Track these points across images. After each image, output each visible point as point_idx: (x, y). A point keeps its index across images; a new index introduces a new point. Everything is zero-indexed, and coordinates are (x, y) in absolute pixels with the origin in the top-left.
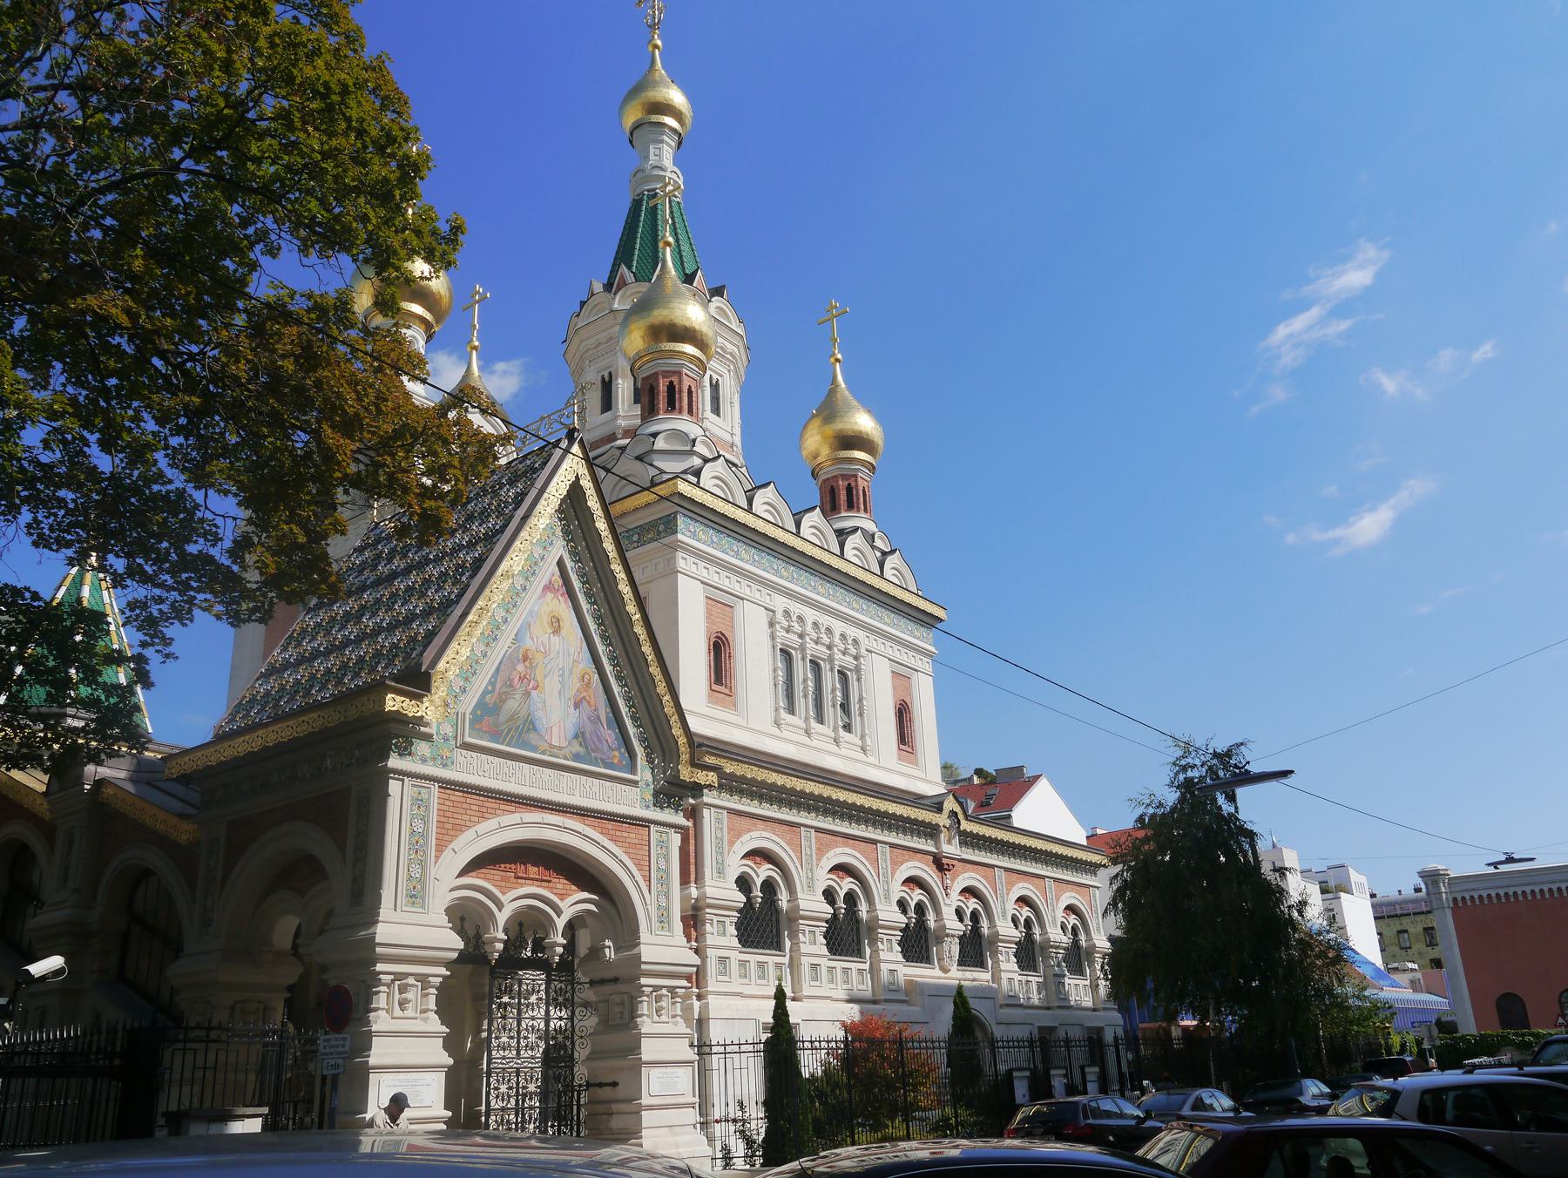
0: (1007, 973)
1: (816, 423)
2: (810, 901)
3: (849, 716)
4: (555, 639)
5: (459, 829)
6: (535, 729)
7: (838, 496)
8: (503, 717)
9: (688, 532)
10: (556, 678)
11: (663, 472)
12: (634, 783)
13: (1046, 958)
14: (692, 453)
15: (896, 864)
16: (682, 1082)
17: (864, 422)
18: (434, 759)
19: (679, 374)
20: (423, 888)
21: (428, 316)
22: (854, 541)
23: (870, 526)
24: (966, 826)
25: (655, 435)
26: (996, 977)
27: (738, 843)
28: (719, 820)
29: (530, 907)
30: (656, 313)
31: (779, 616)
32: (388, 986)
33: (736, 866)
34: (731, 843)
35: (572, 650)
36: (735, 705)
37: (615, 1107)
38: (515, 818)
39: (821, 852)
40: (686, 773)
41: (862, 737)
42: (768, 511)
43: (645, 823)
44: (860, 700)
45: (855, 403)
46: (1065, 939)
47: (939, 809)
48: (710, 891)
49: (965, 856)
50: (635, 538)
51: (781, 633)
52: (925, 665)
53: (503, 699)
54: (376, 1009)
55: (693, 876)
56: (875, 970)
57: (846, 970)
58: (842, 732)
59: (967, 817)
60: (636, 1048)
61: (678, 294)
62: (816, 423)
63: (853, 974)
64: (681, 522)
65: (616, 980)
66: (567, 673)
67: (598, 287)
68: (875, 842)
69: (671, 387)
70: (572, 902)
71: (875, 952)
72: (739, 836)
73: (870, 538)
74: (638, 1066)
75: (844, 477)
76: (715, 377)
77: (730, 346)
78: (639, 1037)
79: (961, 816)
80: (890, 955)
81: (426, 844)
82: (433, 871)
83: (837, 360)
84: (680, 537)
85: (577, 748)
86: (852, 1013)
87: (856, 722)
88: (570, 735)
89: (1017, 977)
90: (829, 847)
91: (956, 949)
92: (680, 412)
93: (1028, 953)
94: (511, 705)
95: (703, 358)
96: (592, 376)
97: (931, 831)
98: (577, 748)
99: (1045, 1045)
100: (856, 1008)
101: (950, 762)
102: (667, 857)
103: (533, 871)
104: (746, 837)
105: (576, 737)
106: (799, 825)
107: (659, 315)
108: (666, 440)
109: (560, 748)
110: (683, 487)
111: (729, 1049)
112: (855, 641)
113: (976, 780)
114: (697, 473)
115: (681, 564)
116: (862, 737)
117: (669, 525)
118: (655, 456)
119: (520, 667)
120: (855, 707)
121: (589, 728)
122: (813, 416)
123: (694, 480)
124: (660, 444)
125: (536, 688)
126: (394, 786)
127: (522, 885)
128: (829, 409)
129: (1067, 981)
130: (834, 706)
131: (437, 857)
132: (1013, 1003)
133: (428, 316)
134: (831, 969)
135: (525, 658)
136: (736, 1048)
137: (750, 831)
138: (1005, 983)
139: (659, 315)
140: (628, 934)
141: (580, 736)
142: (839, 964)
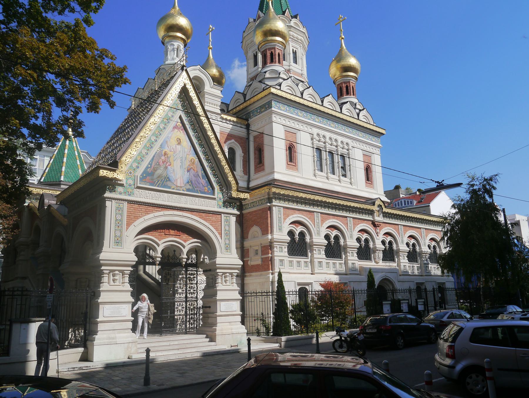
0: (403, 262)
1: (334, 63)
2: (318, 238)
3: (345, 172)
4: (179, 147)
5: (137, 218)
6: (169, 180)
7: (343, 90)
8: (155, 176)
9: (276, 107)
10: (179, 161)
11: (268, 85)
12: (214, 199)
13: (421, 258)
14: (279, 77)
15: (355, 225)
16: (236, 307)
17: (353, 61)
18: (125, 193)
19: (274, 48)
20: (121, 240)
21: (183, 37)
22: (345, 107)
23: (355, 100)
24: (385, 210)
25: (265, 72)
26: (399, 265)
27: (288, 219)
28: (279, 211)
29: (172, 245)
30: (264, 26)
31: (315, 136)
32: (108, 274)
33: (287, 228)
34: (285, 219)
35: (186, 150)
37: (210, 315)
38: (162, 213)
39: (323, 221)
40: (234, 194)
41: (350, 179)
42: (310, 97)
43: (220, 213)
44: (350, 166)
45: (349, 54)
46: (429, 251)
47: (374, 204)
48: (275, 236)
49: (385, 221)
50: (259, 111)
51: (316, 142)
52: (378, 151)
53: (155, 170)
54: (103, 283)
55: (270, 231)
56: (346, 263)
57: (334, 264)
58: (342, 178)
59: (385, 207)
60: (215, 295)
61: (274, 18)
62: (334, 63)
63: (338, 265)
64: (273, 103)
65: (210, 270)
66: (184, 159)
67: (251, 20)
68: (346, 217)
69: (272, 54)
70: (188, 243)
71: (346, 257)
72: (288, 216)
73: (354, 105)
74: (216, 301)
75: (345, 83)
76: (295, 49)
77: (300, 37)
78: (216, 291)
79: (383, 206)
80: (353, 259)
81: (122, 224)
82: (125, 233)
83: (342, 38)
84: (273, 109)
85: (188, 187)
86: (335, 279)
87: (348, 173)
88: (186, 181)
89: (407, 265)
90: (326, 219)
91: (381, 255)
92: (275, 63)
93: (413, 256)
95: (284, 41)
96: (251, 55)
97: (371, 212)
98: (188, 187)
99: (420, 289)
100: (337, 276)
101: (409, 187)
102: (229, 226)
103: (172, 232)
104: (291, 217)
105: (188, 182)
106: (314, 212)
107: (267, 27)
108: (269, 73)
109: (181, 187)
110: (273, 90)
111: (258, 294)
112: (347, 144)
113: (418, 193)
114: (280, 85)
115: (274, 119)
116: (350, 179)
117: (269, 105)
118: (265, 80)
119: (163, 158)
120: (347, 168)
121: (194, 179)
122: (333, 60)
123: (279, 88)
124: (267, 75)
125: (170, 165)
126: (108, 203)
127: (168, 237)
128: (339, 57)
129: (430, 266)
130: (339, 168)
131: (127, 228)
132: (406, 274)
133: (183, 37)
134: (327, 263)
135: (165, 154)
136: (260, 294)
138: (402, 267)
139: (267, 27)
140: (213, 254)
141: (190, 182)
142: (331, 261)
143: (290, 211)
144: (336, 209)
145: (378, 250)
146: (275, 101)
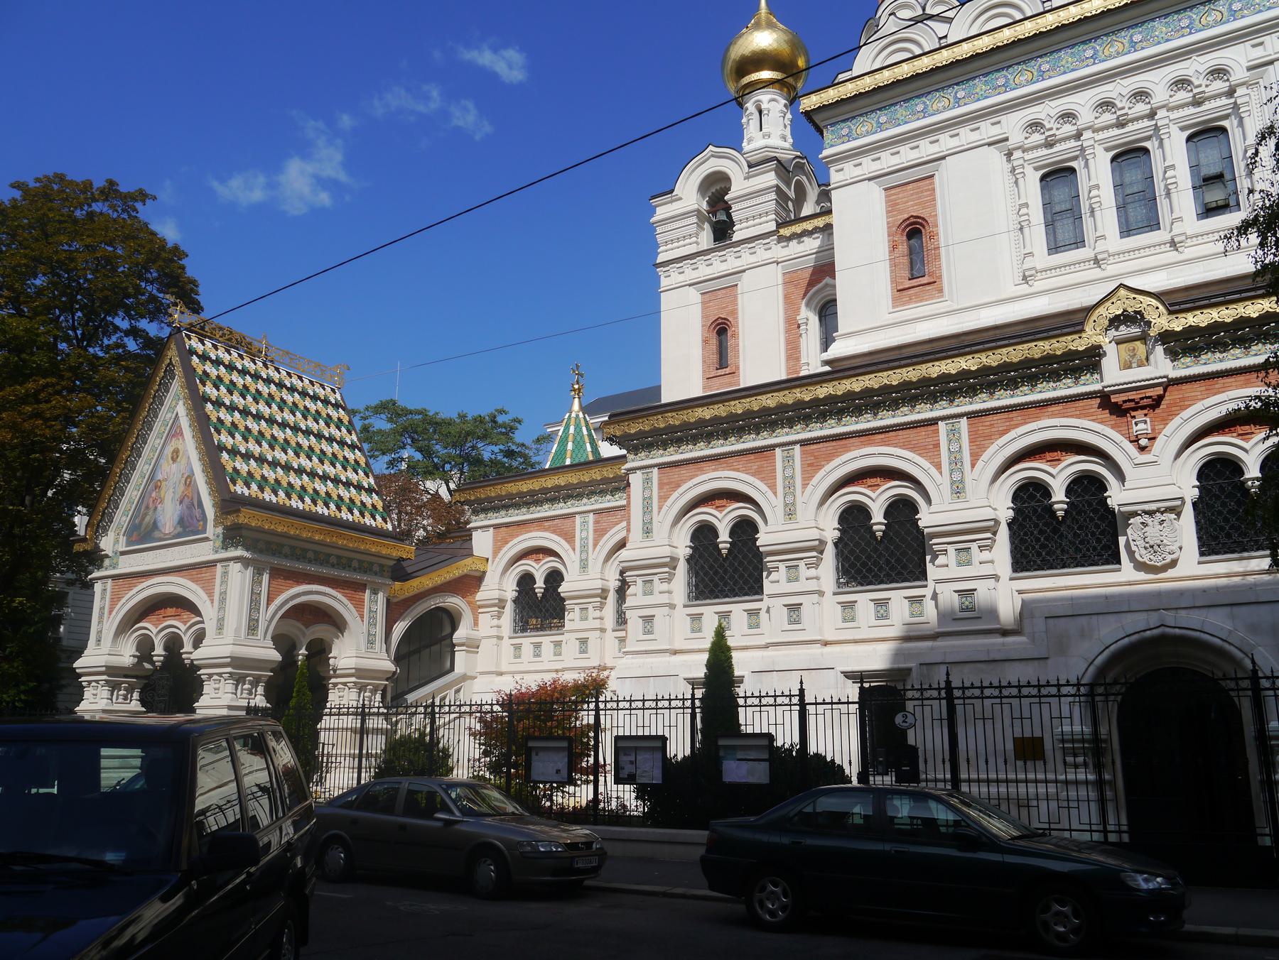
28: (647, 481)
31: (1016, 138)
34: (663, 499)
36: (941, 291)
53: (143, 519)
72: (679, 486)
79: (1150, 316)
90: (829, 458)
94: (148, 519)
137: (692, 478)
143: (683, 471)
144: (840, 414)
145: (1135, 514)
146: (833, 125)
